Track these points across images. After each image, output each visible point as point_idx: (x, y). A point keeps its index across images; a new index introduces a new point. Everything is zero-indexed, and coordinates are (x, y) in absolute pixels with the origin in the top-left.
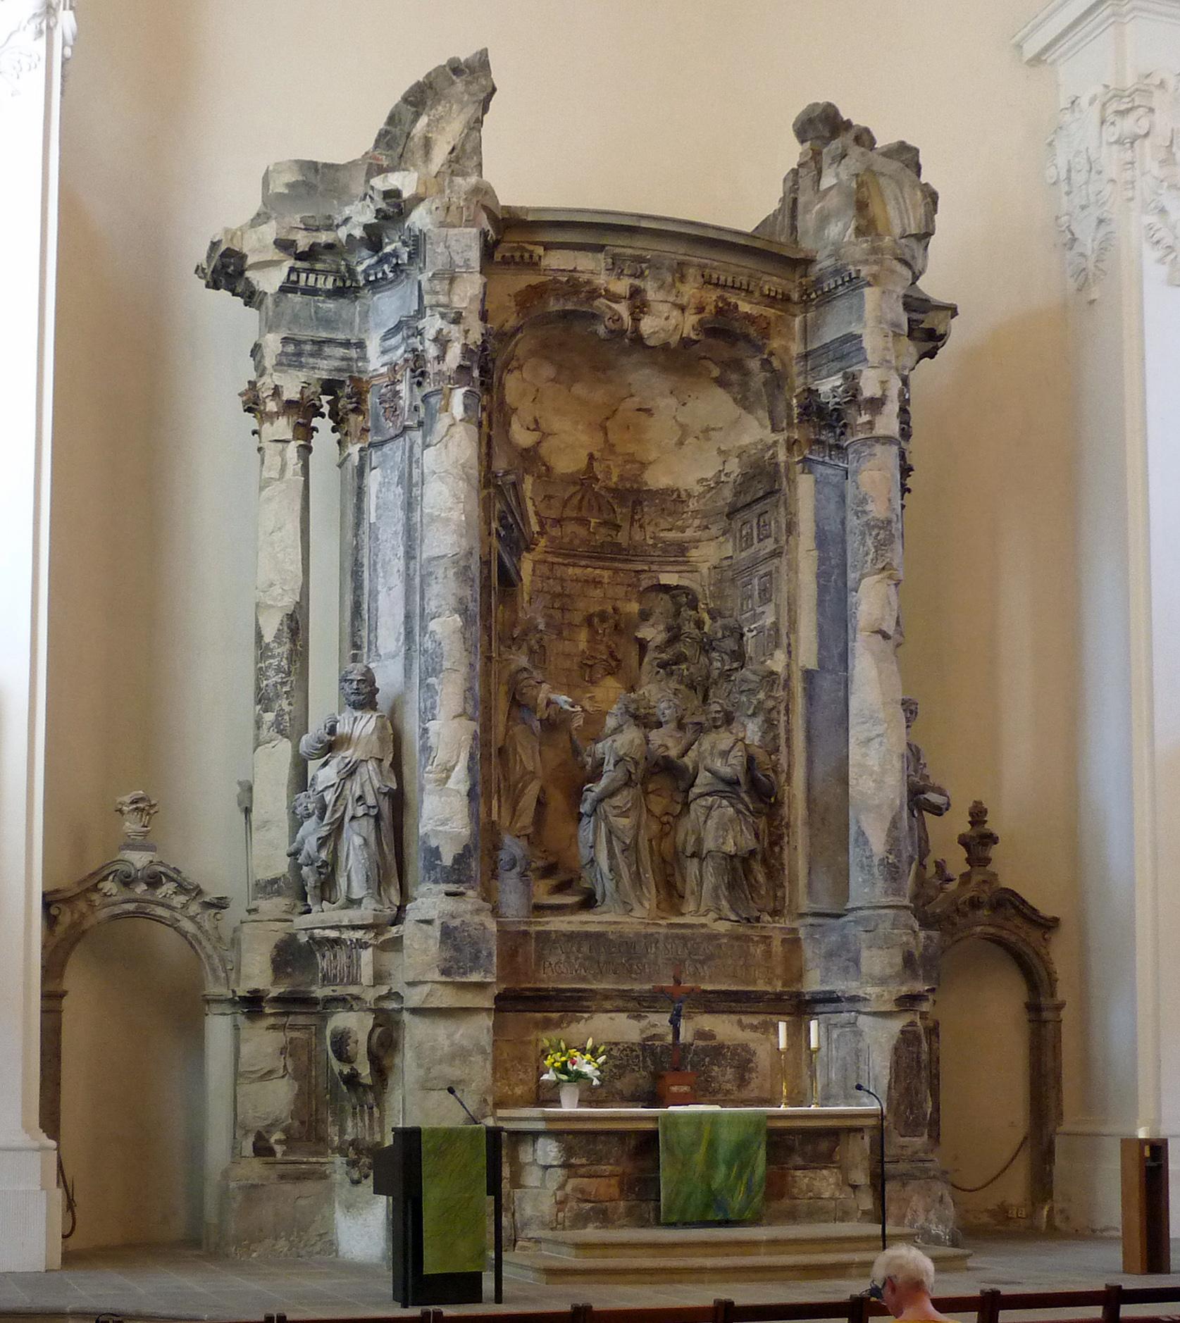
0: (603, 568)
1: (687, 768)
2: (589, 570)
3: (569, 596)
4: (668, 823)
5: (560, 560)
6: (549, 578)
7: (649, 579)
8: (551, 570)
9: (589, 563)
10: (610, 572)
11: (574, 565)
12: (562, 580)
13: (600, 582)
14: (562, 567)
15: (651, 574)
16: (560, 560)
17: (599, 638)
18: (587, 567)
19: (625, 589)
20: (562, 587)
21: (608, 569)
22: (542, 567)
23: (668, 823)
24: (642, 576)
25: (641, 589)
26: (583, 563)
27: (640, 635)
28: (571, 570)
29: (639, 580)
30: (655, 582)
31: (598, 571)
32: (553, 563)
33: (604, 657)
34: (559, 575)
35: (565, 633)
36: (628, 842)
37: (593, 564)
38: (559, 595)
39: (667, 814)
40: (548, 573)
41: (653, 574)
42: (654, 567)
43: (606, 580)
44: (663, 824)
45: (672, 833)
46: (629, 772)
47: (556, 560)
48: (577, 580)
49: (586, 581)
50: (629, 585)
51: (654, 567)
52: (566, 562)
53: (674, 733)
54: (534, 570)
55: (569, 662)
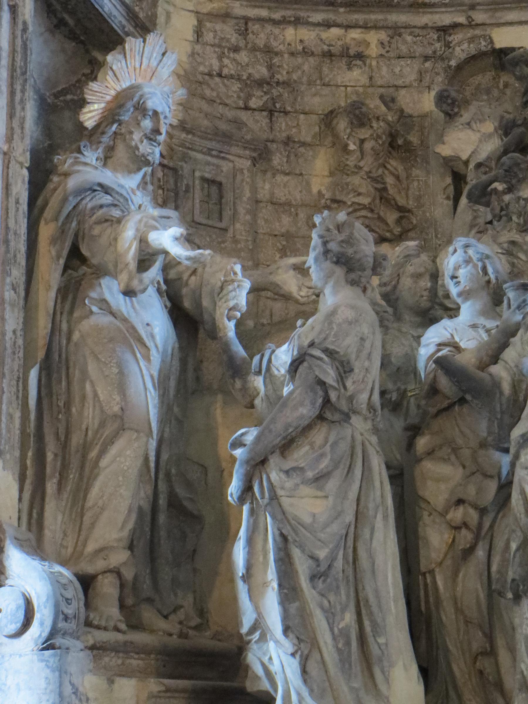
0: (366, 27)
1: (496, 384)
2: (335, 31)
3: (285, 84)
4: (465, 525)
5: (264, 13)
6: (236, 49)
7: (471, 40)
8: (244, 33)
9: (331, 16)
10: (383, 35)
11: (297, 22)
12: (268, 50)
13: (360, 56)
14: (269, 28)
15: (471, 33)
16: (264, 13)
17: (352, 161)
18: (327, 25)
19: (416, 65)
20: (270, 67)
21: (376, 27)
22: (219, 27)
23: (465, 525)
24: (456, 37)
25: (453, 63)
26: (317, 17)
27: (445, 150)
28: (290, 33)
29: (448, 45)
30: (483, 45)
31: (355, 34)
32: (247, 20)
33: (366, 201)
34: (261, 42)
35: (277, 160)
36: (322, 554)
37: (339, 20)
38: (260, 83)
39: (460, 502)
40: (234, 38)
41: (478, 32)
42: (479, 17)
43: (374, 50)
44: (457, 528)
45: (481, 553)
46: (322, 383)
47: (252, 13)
48: (306, 52)
49: (329, 55)
50: (427, 58)
51: (479, 17)
52: (277, 16)
53: (482, 321)
54: (199, 33)
55: (286, 220)
